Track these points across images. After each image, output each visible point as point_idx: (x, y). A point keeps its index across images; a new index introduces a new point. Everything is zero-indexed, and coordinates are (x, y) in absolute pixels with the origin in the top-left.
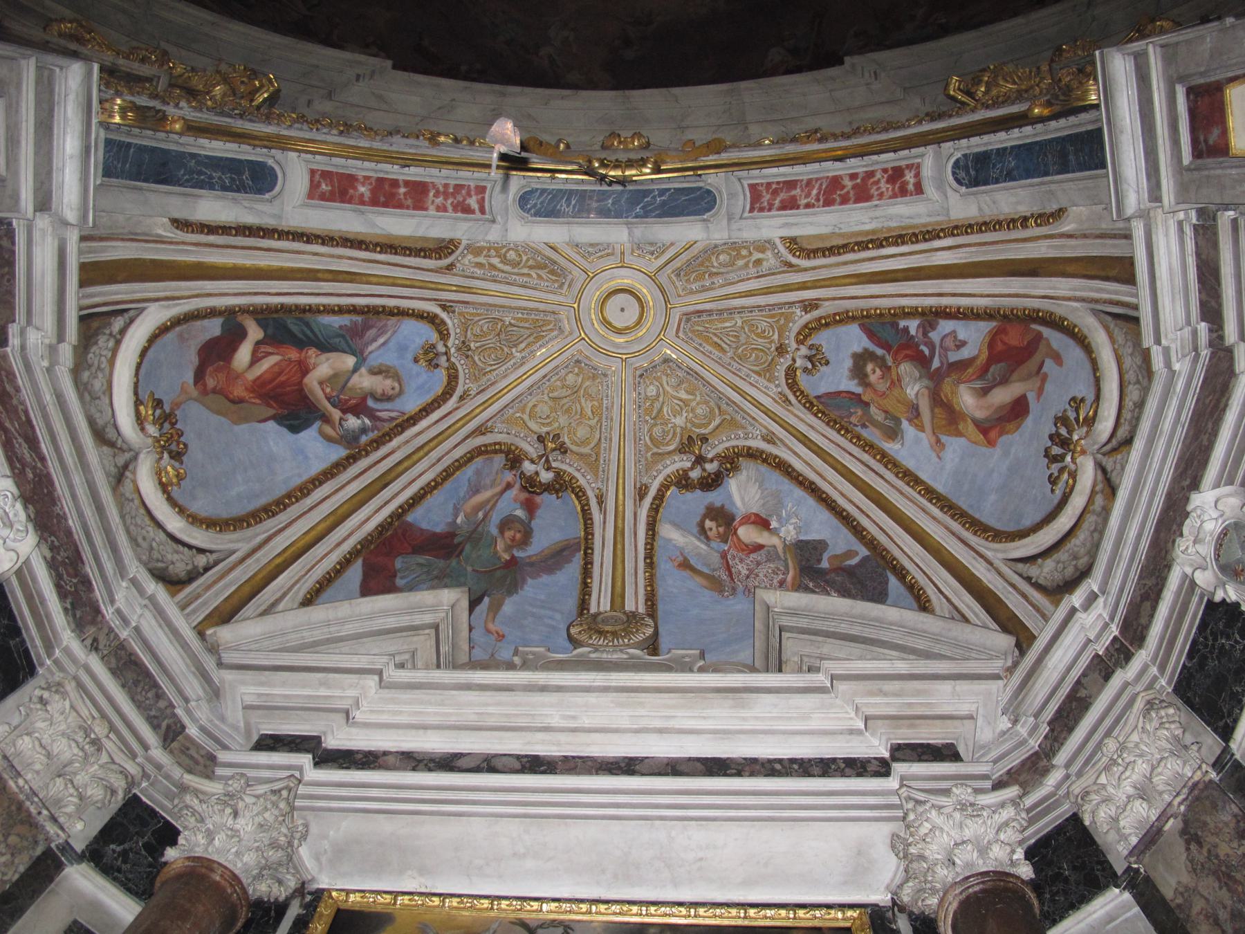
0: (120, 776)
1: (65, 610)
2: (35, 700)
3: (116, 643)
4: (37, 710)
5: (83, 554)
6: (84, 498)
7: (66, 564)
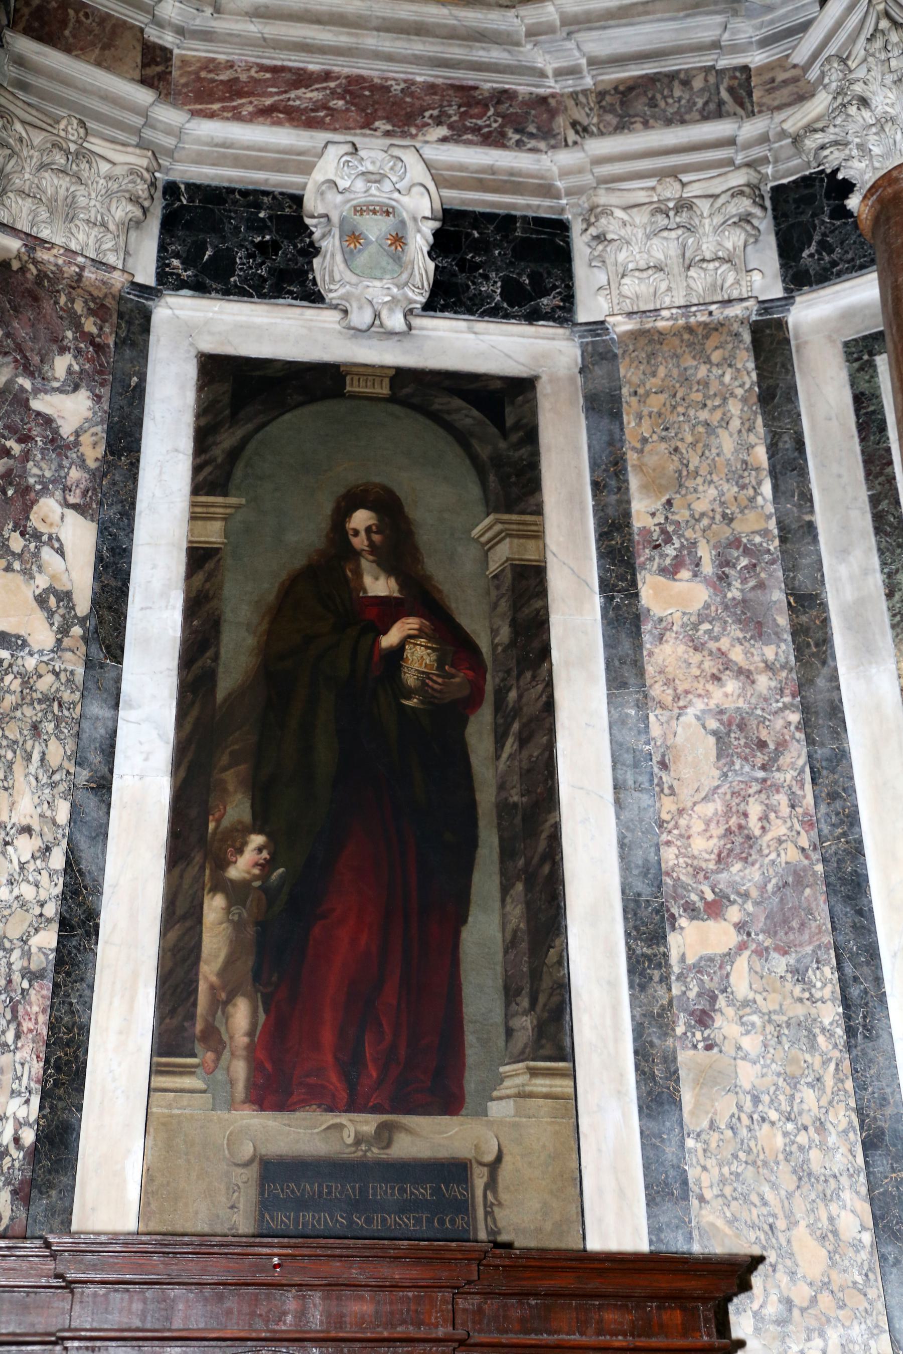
0: (736, 200)
1: (519, 144)
2: (594, 244)
3: (592, 98)
4: (604, 250)
5: (465, 83)
6: (399, 44)
7: (465, 113)
